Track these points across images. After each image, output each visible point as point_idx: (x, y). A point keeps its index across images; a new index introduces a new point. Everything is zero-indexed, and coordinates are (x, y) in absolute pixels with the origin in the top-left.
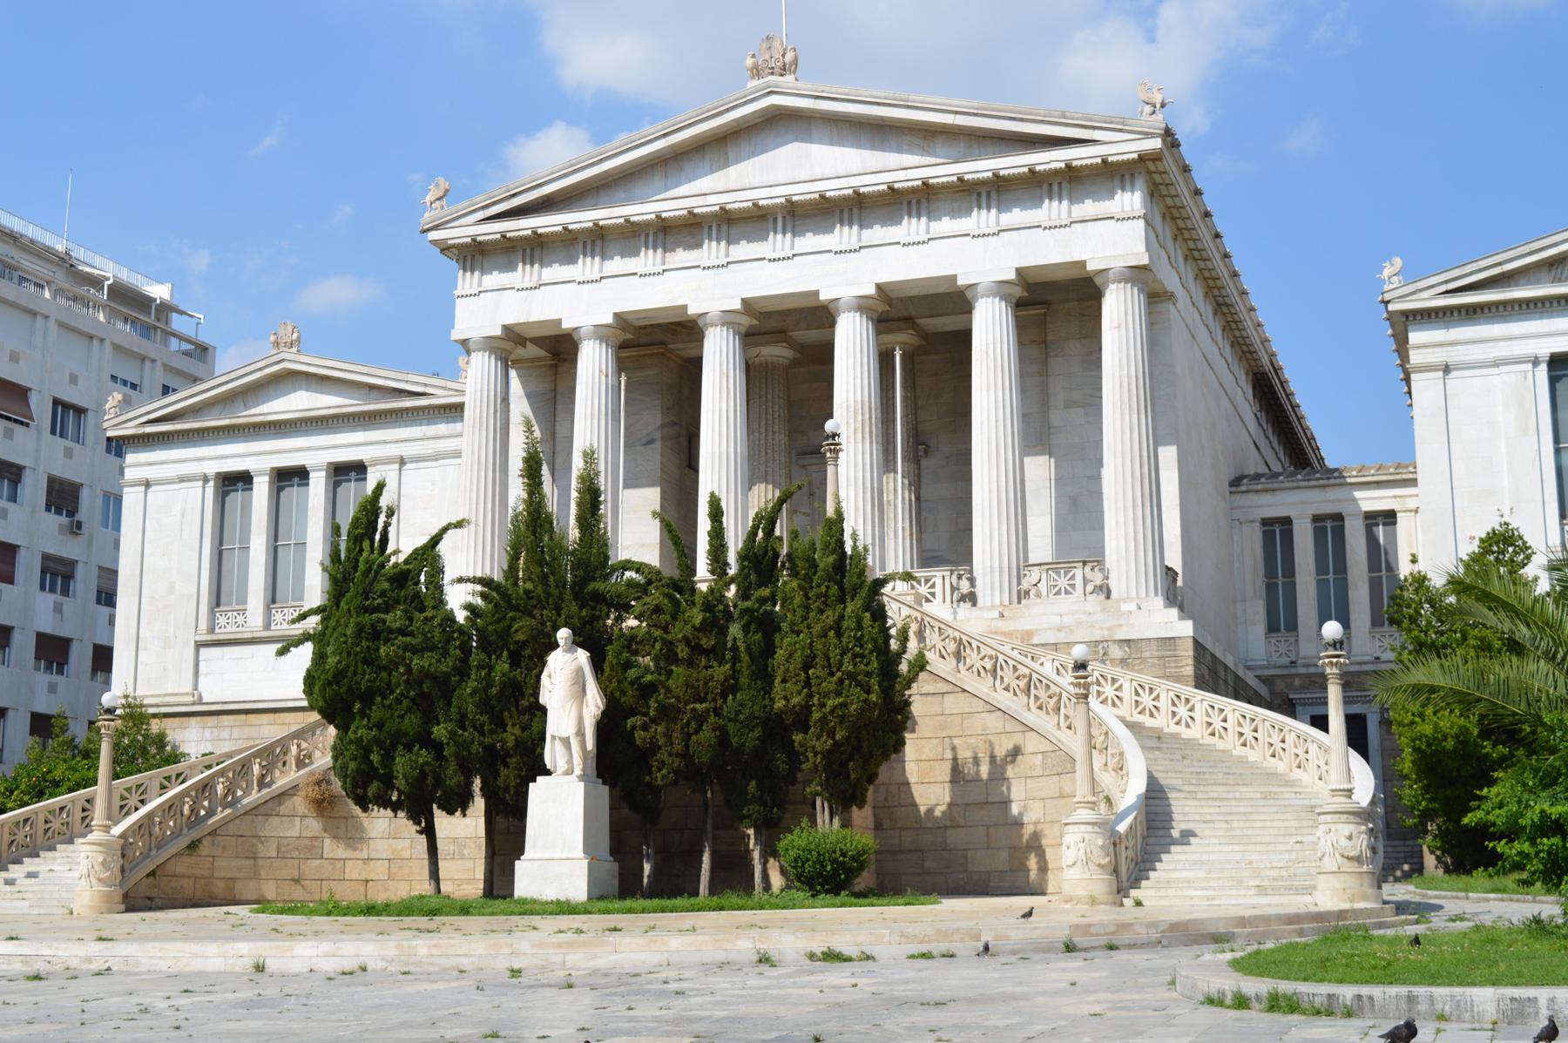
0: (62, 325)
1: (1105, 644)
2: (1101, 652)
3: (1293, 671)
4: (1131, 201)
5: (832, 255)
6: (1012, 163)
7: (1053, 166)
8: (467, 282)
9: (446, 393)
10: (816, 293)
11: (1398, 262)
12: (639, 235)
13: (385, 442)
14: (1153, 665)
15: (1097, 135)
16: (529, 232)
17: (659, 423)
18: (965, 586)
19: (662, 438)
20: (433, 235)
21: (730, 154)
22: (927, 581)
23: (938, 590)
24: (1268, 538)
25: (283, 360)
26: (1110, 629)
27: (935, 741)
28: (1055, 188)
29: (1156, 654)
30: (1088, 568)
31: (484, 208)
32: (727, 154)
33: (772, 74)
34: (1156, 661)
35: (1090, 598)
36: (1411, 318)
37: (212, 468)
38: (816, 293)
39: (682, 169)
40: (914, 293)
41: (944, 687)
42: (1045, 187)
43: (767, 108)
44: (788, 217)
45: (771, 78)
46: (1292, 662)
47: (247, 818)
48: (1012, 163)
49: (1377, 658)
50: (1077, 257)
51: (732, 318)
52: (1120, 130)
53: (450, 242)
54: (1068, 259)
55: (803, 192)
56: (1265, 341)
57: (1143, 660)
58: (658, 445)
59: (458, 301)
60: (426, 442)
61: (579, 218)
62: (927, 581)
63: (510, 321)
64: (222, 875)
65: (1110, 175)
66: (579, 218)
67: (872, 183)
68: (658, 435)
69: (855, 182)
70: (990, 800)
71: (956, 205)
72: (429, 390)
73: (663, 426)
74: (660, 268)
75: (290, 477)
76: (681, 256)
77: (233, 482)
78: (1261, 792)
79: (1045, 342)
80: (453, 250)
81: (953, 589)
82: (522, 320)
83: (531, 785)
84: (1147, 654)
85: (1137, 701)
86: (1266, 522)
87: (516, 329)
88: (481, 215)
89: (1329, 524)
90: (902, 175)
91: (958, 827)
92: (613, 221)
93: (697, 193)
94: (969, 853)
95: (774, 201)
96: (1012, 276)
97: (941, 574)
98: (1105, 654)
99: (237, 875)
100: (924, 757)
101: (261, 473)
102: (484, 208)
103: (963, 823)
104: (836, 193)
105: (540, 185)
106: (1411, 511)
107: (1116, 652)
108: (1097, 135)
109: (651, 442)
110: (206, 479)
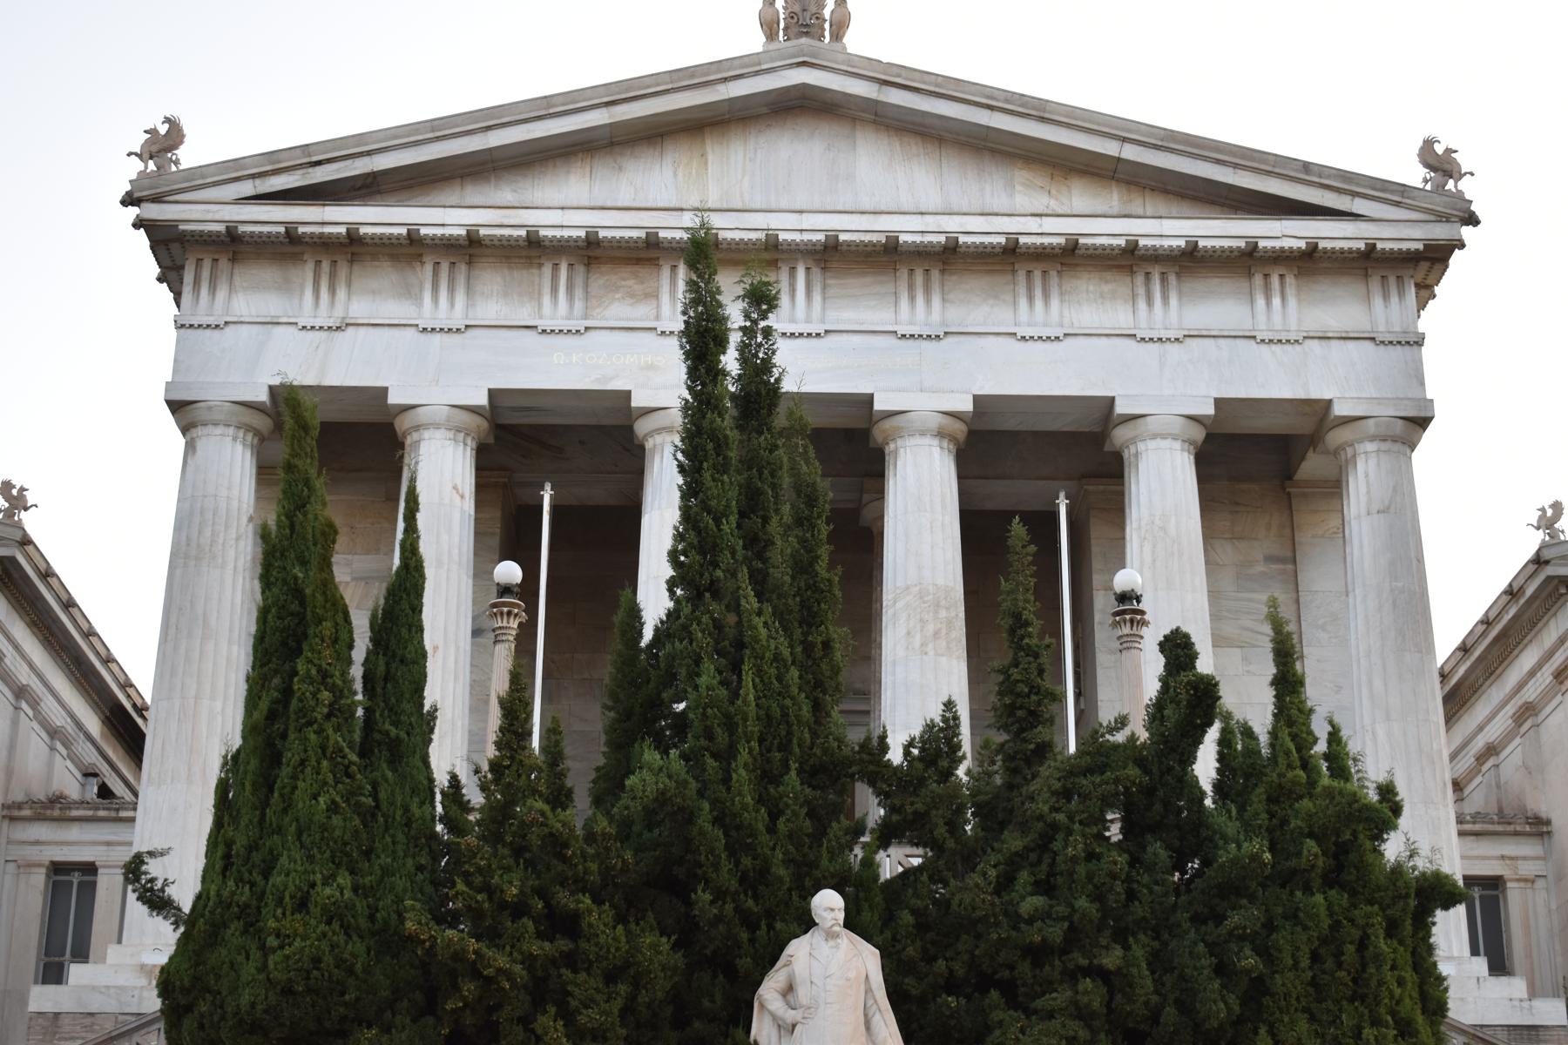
5: (892, 340)
15: (1359, 206)
21: (710, 157)
31: (253, 176)
33: (807, 34)
39: (620, 168)
43: (805, 86)
45: (804, 40)
50: (1315, 394)
52: (1397, 204)
53: (182, 227)
54: (1300, 394)
55: (854, 228)
69: (953, 224)
71: (1106, 288)
74: (581, 324)
88: (247, 188)
90: (1032, 225)
92: (506, 232)
93: (660, 205)
102: (253, 176)
105: (369, 153)
106: (1526, 880)
108: (1359, 206)
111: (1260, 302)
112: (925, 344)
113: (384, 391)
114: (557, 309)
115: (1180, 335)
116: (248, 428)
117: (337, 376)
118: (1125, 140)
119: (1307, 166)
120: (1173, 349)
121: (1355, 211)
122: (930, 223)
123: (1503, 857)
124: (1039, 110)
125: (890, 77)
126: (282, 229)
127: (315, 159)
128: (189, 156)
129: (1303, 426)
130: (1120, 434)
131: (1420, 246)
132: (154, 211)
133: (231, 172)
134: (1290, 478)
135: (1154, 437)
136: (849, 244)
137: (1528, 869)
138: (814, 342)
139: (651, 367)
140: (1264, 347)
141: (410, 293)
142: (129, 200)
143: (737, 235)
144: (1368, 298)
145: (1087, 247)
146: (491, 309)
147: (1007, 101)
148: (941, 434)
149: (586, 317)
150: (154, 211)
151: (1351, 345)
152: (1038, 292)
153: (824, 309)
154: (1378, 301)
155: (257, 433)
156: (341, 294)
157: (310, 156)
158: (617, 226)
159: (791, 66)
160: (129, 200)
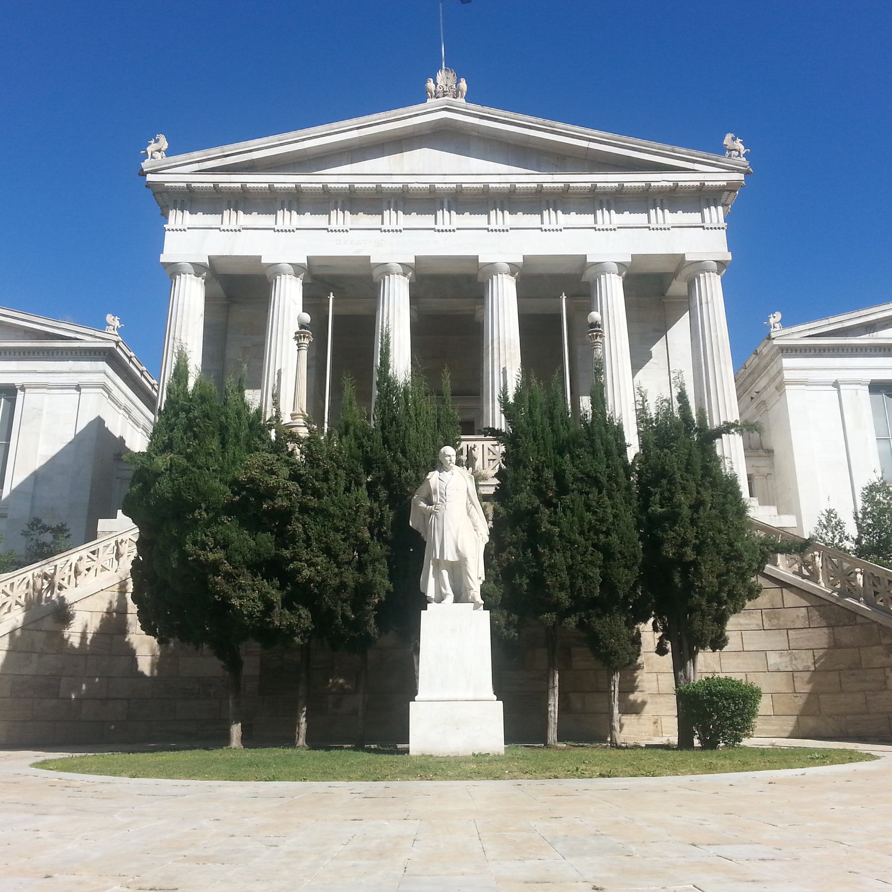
4: (716, 215)
8: (177, 219)
9: (95, 340)
11: (778, 316)
12: (329, 202)
13: (36, 372)
20: (150, 178)
28: (658, 202)
53: (166, 185)
59: (167, 232)
60: (71, 375)
61: (285, 181)
66: (285, 181)
72: (78, 336)
80: (165, 195)
88: (196, 167)
95: (448, 186)
121: (695, 169)
126: (212, 185)
127: (226, 153)
129: (671, 268)
130: (589, 273)
131: (725, 183)
134: (664, 295)
136: (467, 188)
137: (765, 470)
143: (417, 186)
145: (574, 188)
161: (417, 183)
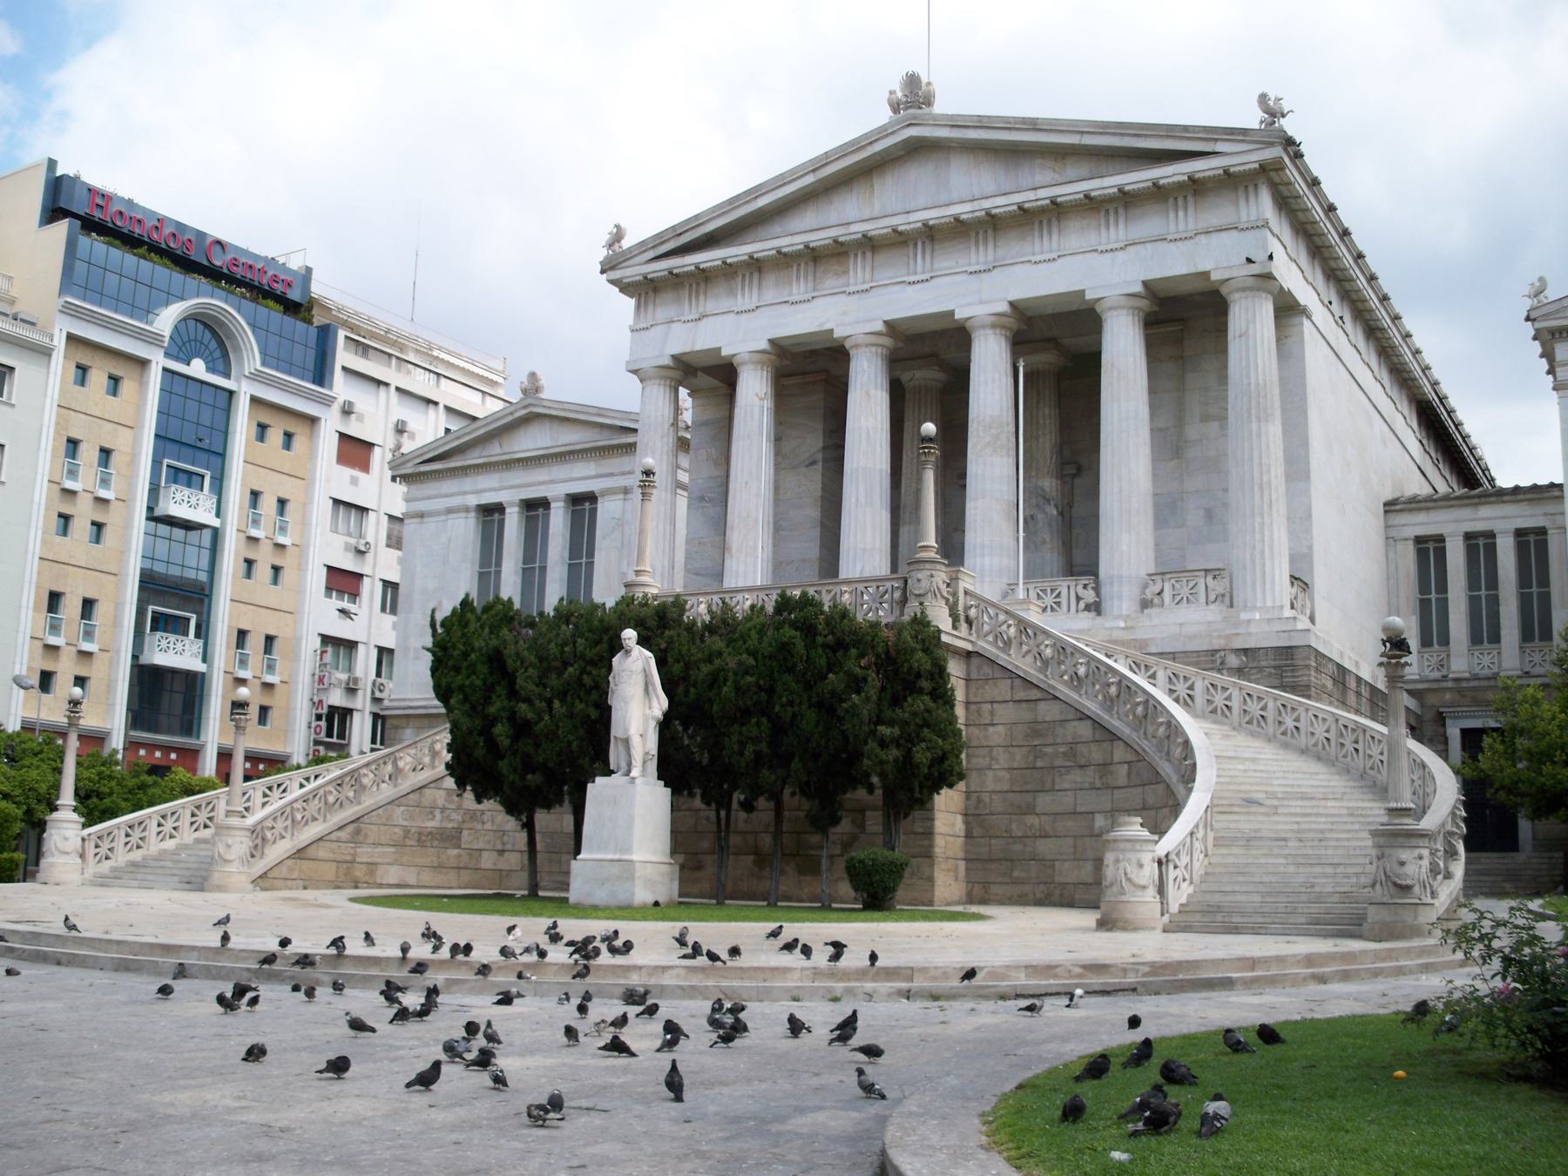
0: (398, 389)
1: (1222, 653)
2: (1219, 661)
3: (1444, 685)
5: (965, 277)
6: (1137, 178)
7: (1176, 179)
10: (952, 313)
14: (1270, 675)
15: (1219, 147)
16: (693, 268)
17: (821, 445)
18: (1089, 595)
19: (825, 460)
21: (876, 187)
22: (1052, 591)
23: (1064, 600)
24: (1422, 555)
25: (530, 405)
26: (1228, 637)
27: (1024, 750)
29: (1273, 663)
30: (1210, 578)
31: (653, 247)
32: (872, 186)
34: (1273, 671)
35: (1212, 607)
36: (1557, 336)
37: (473, 501)
38: (952, 313)
40: (1049, 311)
41: (1035, 694)
42: (1171, 200)
44: (927, 242)
46: (1444, 677)
47: (389, 807)
48: (1137, 178)
49: (1527, 673)
50: (1201, 268)
51: (874, 339)
52: (1242, 141)
54: (1193, 270)
56: (1426, 369)
57: (1260, 669)
58: (819, 466)
62: (1052, 591)
63: (677, 350)
64: (365, 859)
65: (1232, 182)
67: (1002, 204)
68: (820, 456)
69: (987, 204)
70: (1079, 810)
71: (1085, 222)
73: (824, 448)
74: (809, 296)
75: (535, 508)
76: (831, 283)
77: (491, 513)
78: (1348, 808)
79: (1182, 358)
81: (1078, 599)
82: (688, 350)
83: (589, 785)
84: (1264, 663)
85: (1245, 711)
86: (1419, 540)
87: (684, 359)
88: (651, 254)
89: (1481, 542)
90: (1031, 195)
91: (1046, 837)
94: (1057, 863)
96: (1139, 288)
97: (1066, 583)
98: (1222, 663)
99: (379, 860)
100: (1015, 765)
101: (512, 504)
102: (653, 247)
103: (1052, 833)
104: (970, 216)
107: (1233, 661)
109: (813, 463)
110: (467, 509)
111: (1172, 215)
112: (983, 276)
113: (719, 349)
114: (799, 289)
115: (1122, 245)
116: (665, 378)
117: (701, 345)
118: (1083, 133)
119: (1186, 128)
120: (1120, 254)
122: (976, 205)
123: (1545, 514)
124: (1033, 125)
125: (956, 122)
128: (626, 243)
132: (616, 274)
133: (643, 246)
135: (1111, 309)
138: (926, 284)
139: (845, 313)
140: (1172, 244)
141: (732, 293)
142: (603, 272)
144: (1236, 203)
146: (770, 294)
147: (1016, 123)
148: (993, 326)
149: (814, 290)
150: (616, 274)
151: (1224, 235)
152: (1045, 232)
153: (932, 263)
154: (1242, 203)
155: (672, 379)
156: (702, 298)
157: (676, 231)
158: (818, 239)
159: (903, 128)
160: (603, 272)
161: (876, 228)
